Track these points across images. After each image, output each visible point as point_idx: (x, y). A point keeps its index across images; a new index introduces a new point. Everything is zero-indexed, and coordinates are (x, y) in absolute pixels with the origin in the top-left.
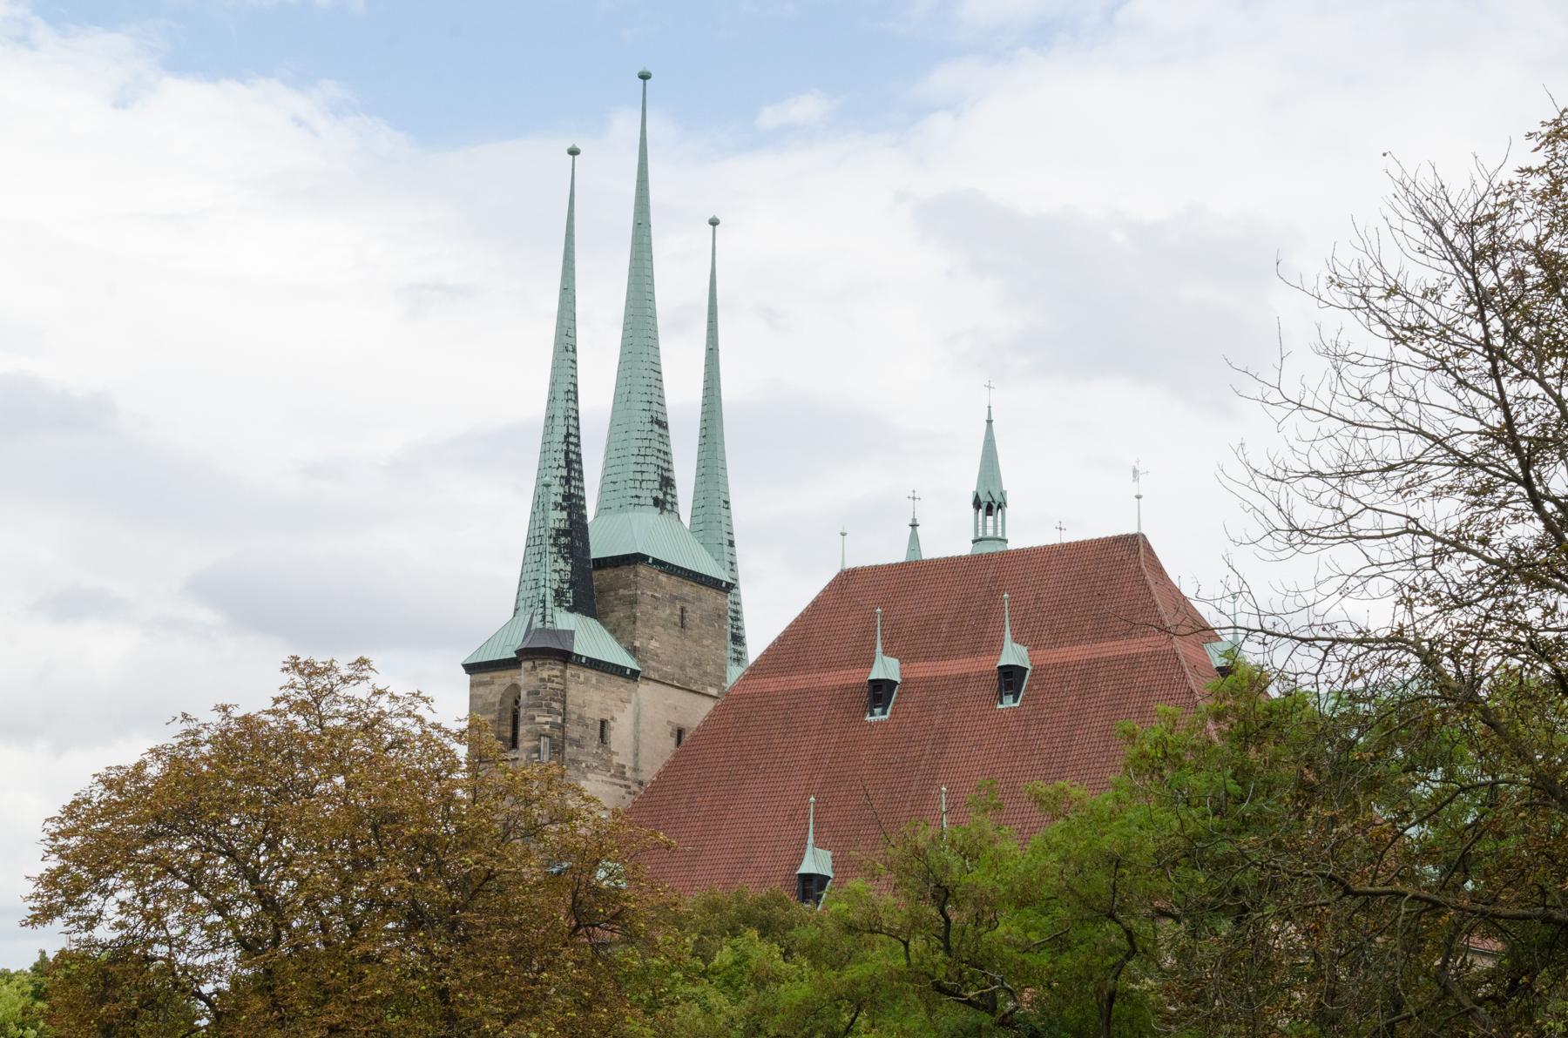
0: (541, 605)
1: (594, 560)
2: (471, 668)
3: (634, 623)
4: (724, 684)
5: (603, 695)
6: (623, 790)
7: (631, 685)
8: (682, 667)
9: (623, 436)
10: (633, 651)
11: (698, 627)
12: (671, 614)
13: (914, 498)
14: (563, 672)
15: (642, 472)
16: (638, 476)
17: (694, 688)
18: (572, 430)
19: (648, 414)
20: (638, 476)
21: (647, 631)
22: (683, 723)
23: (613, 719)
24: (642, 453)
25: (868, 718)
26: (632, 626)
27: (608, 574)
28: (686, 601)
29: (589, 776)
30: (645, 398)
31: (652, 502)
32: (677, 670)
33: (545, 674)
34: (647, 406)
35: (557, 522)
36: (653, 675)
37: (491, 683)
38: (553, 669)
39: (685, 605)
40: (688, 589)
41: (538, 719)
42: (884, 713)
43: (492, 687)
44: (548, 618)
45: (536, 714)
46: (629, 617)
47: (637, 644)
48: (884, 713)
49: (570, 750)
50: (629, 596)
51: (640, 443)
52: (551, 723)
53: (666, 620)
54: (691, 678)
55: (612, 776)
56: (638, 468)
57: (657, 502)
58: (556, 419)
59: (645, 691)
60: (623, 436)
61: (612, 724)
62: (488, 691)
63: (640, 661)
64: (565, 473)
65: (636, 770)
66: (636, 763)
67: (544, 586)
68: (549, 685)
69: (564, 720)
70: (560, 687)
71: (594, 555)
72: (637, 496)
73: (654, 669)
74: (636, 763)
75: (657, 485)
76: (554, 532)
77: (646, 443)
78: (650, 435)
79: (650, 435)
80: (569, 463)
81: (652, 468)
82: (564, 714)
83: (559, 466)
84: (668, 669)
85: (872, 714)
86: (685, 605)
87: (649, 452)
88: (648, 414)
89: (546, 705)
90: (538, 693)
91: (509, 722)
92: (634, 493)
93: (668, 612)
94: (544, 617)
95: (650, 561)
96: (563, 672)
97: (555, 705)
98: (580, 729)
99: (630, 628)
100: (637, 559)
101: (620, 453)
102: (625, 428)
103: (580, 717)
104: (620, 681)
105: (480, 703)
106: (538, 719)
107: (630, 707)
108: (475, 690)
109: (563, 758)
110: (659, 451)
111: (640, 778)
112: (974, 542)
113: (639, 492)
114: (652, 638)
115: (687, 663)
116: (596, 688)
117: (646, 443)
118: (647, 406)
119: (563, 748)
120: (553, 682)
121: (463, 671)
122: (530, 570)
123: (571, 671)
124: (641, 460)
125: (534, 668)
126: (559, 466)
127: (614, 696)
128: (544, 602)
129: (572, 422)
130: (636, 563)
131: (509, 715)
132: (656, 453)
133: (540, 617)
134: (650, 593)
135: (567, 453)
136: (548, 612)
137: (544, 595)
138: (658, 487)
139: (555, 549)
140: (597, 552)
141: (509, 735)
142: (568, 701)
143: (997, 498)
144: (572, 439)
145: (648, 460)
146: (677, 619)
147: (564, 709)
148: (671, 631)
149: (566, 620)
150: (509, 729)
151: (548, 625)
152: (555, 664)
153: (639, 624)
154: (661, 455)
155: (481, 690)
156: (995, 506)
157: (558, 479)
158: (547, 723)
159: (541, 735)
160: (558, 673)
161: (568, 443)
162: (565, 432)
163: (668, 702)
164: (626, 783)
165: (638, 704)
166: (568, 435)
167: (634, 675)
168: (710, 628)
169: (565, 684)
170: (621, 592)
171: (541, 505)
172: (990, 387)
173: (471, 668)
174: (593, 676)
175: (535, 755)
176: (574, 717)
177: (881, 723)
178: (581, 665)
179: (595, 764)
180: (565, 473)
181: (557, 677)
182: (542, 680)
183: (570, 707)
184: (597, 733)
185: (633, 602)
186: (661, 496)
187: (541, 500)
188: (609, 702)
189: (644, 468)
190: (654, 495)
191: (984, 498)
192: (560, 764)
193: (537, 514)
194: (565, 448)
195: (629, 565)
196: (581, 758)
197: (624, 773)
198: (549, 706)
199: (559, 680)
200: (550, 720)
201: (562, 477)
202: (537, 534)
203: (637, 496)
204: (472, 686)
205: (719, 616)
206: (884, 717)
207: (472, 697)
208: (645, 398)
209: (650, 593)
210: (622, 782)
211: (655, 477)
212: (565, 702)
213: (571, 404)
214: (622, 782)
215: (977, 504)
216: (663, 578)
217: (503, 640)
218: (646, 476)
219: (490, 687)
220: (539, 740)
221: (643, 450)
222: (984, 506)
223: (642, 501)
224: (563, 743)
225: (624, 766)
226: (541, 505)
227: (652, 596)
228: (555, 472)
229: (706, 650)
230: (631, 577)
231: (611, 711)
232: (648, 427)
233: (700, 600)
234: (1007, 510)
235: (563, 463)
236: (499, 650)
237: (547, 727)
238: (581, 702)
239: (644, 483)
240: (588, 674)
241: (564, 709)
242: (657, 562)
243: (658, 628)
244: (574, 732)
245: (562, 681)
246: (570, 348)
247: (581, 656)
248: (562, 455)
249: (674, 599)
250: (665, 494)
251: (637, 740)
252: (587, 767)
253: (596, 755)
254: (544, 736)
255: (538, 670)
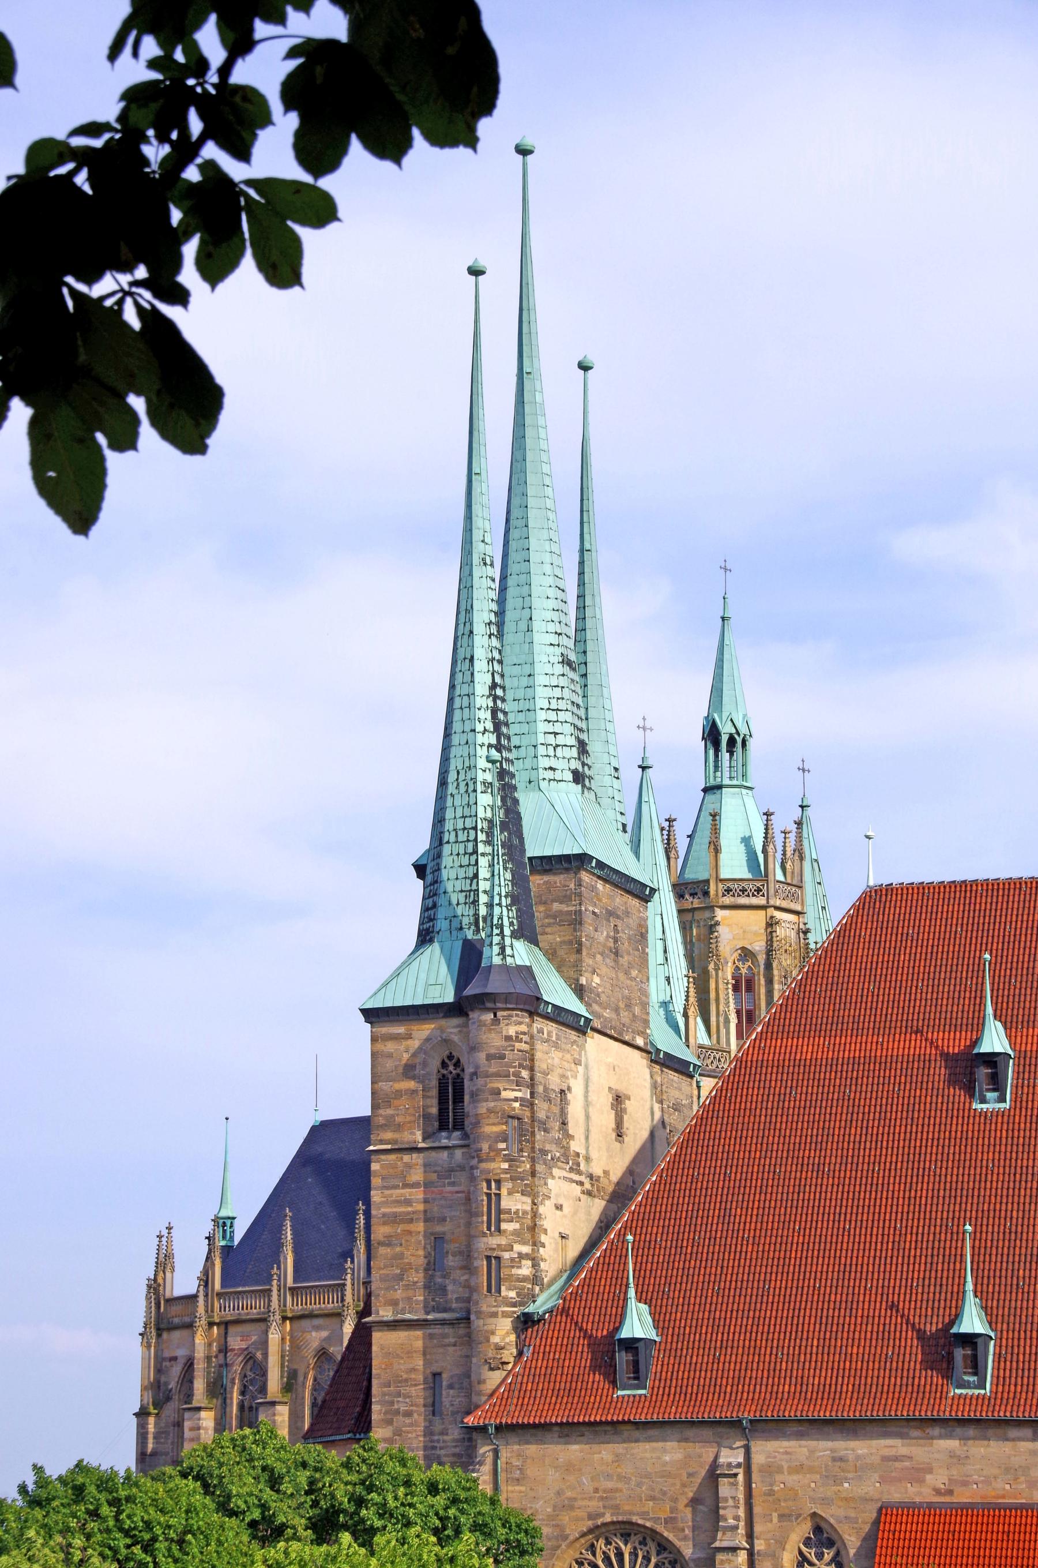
0: (496, 931)
1: (529, 858)
2: (371, 1015)
3: (579, 951)
4: (648, 1031)
5: (560, 1055)
6: (579, 1188)
7: (580, 1040)
8: (617, 1010)
9: (525, 681)
10: (580, 991)
11: (629, 954)
12: (608, 936)
13: (644, 729)
14: (530, 1026)
15: (556, 734)
16: (551, 740)
17: (627, 1038)
18: (498, 679)
19: (558, 651)
20: (551, 740)
21: (591, 962)
22: (621, 1088)
23: (569, 1089)
24: (554, 706)
25: (977, 1106)
26: (578, 956)
27: (536, 882)
28: (618, 917)
29: (556, 1171)
30: (552, 627)
31: (570, 777)
32: (614, 1016)
33: (512, 1031)
34: (554, 639)
35: (489, 810)
36: (597, 1024)
37: (409, 1036)
38: (520, 1023)
39: (619, 923)
40: (621, 900)
41: (505, 1094)
42: (1002, 1099)
43: (409, 1042)
44: (508, 951)
45: (501, 1086)
46: (570, 942)
47: (583, 981)
48: (1002, 1099)
49: (539, 1136)
50: (569, 913)
51: (549, 692)
52: (522, 1099)
53: (604, 946)
54: (624, 1025)
55: (571, 1170)
56: (550, 728)
57: (578, 777)
58: (476, 663)
59: (594, 1043)
60: (525, 681)
61: (569, 1096)
62: (402, 1048)
63: (588, 1005)
64: (494, 741)
65: (588, 1159)
66: (587, 1149)
67: (500, 905)
68: (517, 1045)
69: (532, 1094)
70: (525, 1047)
71: (530, 852)
72: (551, 768)
73: (599, 1016)
74: (587, 1149)
75: (574, 752)
76: (485, 825)
77: (557, 692)
78: (563, 681)
79: (563, 681)
80: (497, 726)
81: (568, 729)
82: (532, 1085)
83: (485, 730)
84: (607, 1014)
85: (983, 1101)
86: (619, 923)
87: (562, 705)
88: (558, 651)
89: (514, 1075)
90: (502, 1057)
91: (435, 1092)
92: (543, 763)
93: (605, 933)
94: (503, 949)
95: (594, 864)
96: (530, 1026)
97: (525, 1074)
98: (545, 1106)
99: (573, 958)
100: (579, 861)
101: (524, 705)
102: (527, 670)
103: (546, 1089)
104: (573, 1035)
105: (389, 1064)
106: (505, 1094)
107: (581, 1069)
108: (380, 1046)
109: (533, 1148)
110: (573, 703)
111: (590, 1171)
112: (705, 790)
113: (553, 763)
114: (594, 972)
115: (622, 1005)
116: (556, 1046)
117: (557, 692)
118: (554, 639)
119: (533, 1134)
120: (521, 1041)
121: (361, 1018)
122: (453, 876)
123: (539, 1024)
124: (552, 716)
125: (496, 1021)
126: (485, 730)
127: (568, 1056)
128: (501, 927)
129: (497, 667)
130: (579, 869)
131: (434, 1083)
132: (569, 707)
133: (496, 949)
134: (591, 908)
135: (494, 712)
136: (508, 941)
137: (501, 918)
138: (576, 755)
139: (488, 849)
140: (534, 849)
141: (434, 1110)
142: (536, 1069)
143: (743, 730)
144: (499, 692)
145: (562, 716)
146: (612, 945)
147: (532, 1078)
148: (608, 961)
149: (521, 953)
150: (435, 1102)
151: (509, 960)
152: (523, 1017)
153: (584, 953)
154: (575, 709)
155: (390, 1047)
156: (739, 740)
157: (485, 748)
158: (516, 1099)
159: (510, 1117)
160: (523, 1028)
161: (495, 698)
162: (489, 682)
163: (609, 1060)
164: (582, 1178)
165: (586, 1067)
166: (494, 686)
167: (588, 1021)
168: (636, 953)
169: (531, 1044)
170: (556, 906)
171: (462, 785)
172: (726, 569)
173: (371, 1015)
174: (550, 1028)
175: (502, 1145)
176: (540, 1089)
177: (997, 1113)
178: (546, 1017)
179: (558, 1154)
180: (493, 739)
181: (524, 1033)
182: (508, 1038)
183: (538, 1076)
184: (556, 1110)
185: (576, 921)
186: (581, 770)
187: (462, 777)
188: (566, 1065)
189: (558, 727)
190: (573, 767)
191: (726, 730)
192: (533, 1160)
193: (457, 798)
194: (491, 704)
195: (567, 870)
196: (548, 1147)
197: (578, 1165)
198: (517, 1075)
199: (525, 1038)
200: (519, 1094)
201: (490, 746)
202: (460, 825)
203: (551, 768)
204: (374, 1039)
205: (642, 934)
206: (1002, 1105)
207: (374, 1055)
208: (552, 627)
209: (591, 908)
210: (576, 1177)
211: (572, 741)
212: (532, 1069)
213: (495, 642)
214: (576, 1177)
215: (712, 735)
216: (600, 885)
217: (423, 976)
218: (560, 740)
219: (405, 1043)
220: (506, 1122)
221: (554, 702)
222: (724, 739)
223: (558, 775)
224: (532, 1128)
225: (578, 1155)
226: (462, 785)
227: (594, 913)
228: (480, 739)
229: (634, 983)
230: (572, 886)
231: (567, 1078)
232: (559, 669)
233: (627, 913)
234: (751, 743)
235: (490, 726)
236: (420, 989)
237: (517, 1105)
238: (545, 1067)
239: (559, 749)
240: (550, 1028)
241: (532, 1078)
242: (601, 865)
243: (599, 957)
244: (542, 1109)
245: (528, 1040)
246: (488, 562)
247: (548, 1003)
248: (488, 715)
249: (611, 914)
250: (584, 764)
251: (587, 1117)
252: (552, 1159)
253: (558, 1142)
254: (512, 1117)
255: (502, 1025)
